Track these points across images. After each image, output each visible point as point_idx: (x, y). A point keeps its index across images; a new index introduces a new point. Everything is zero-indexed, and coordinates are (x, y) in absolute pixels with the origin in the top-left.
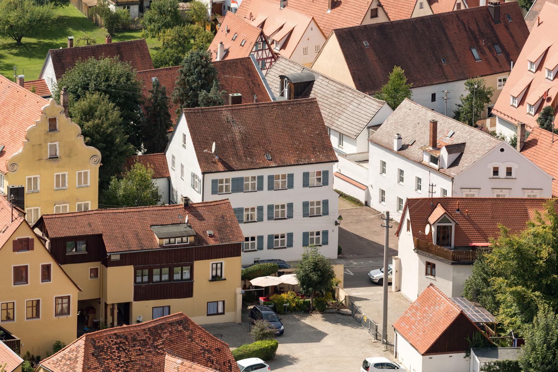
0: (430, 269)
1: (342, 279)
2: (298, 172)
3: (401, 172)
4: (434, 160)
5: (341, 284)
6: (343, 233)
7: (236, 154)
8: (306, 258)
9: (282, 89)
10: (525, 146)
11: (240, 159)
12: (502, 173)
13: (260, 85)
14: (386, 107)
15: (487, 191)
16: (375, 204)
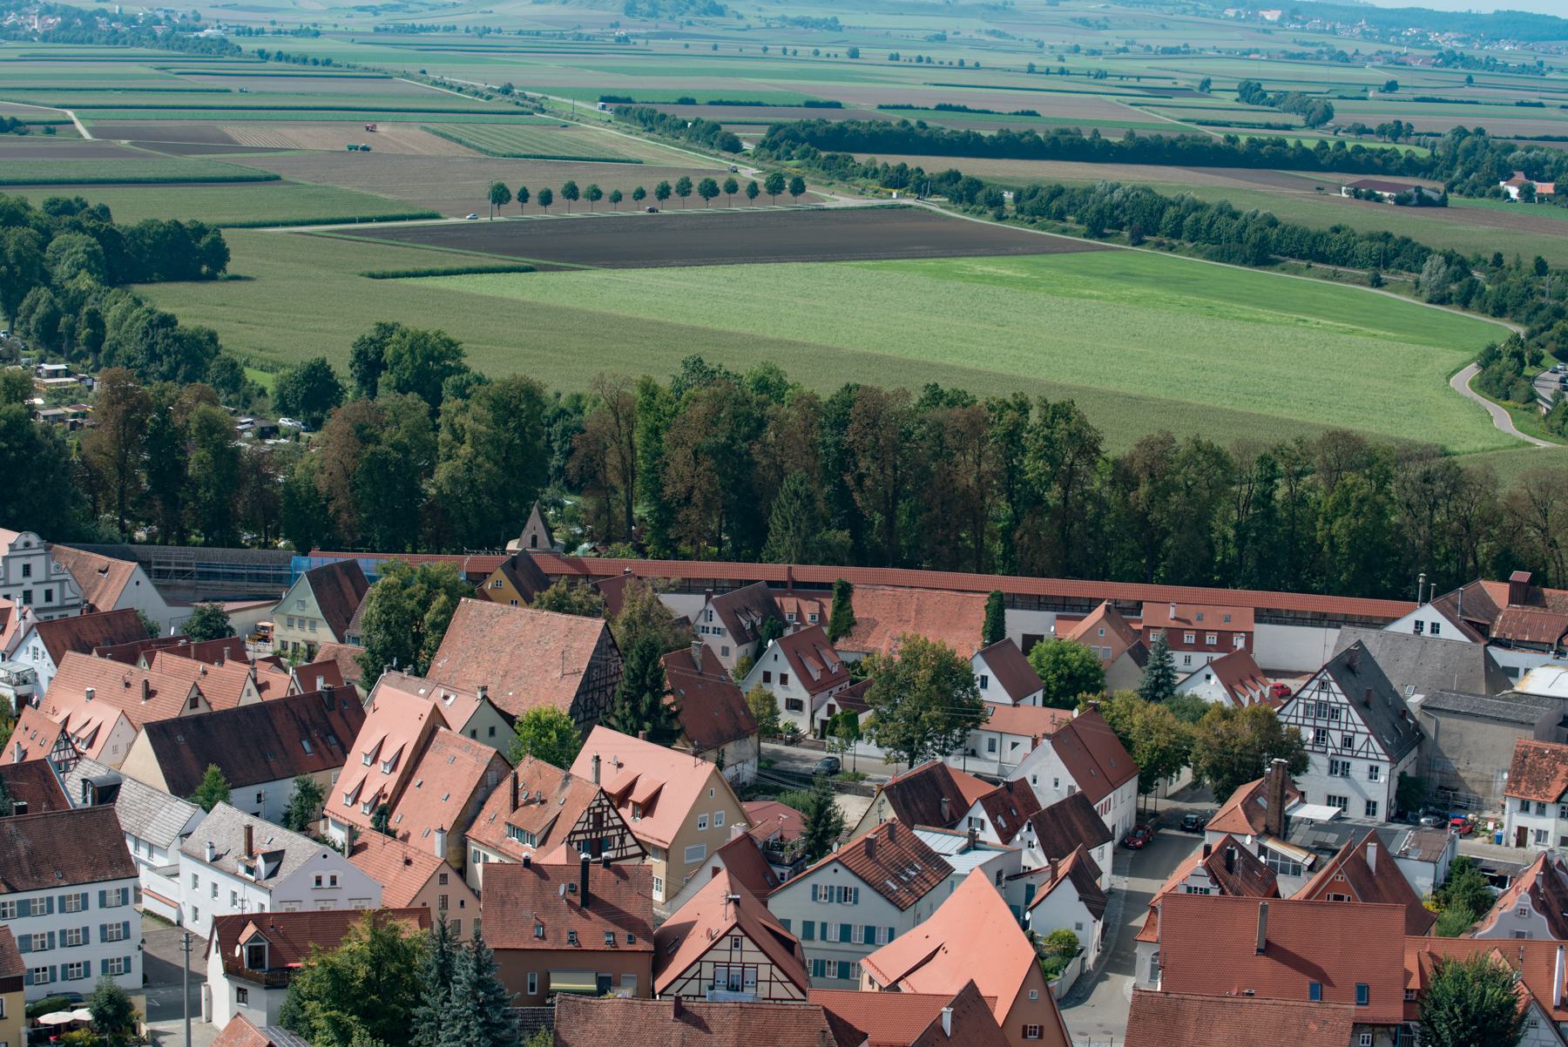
0: (241, 995)
1: (144, 1011)
2: (93, 891)
3: (215, 886)
4: (250, 870)
5: (144, 1017)
6: (148, 960)
7: (21, 873)
8: (99, 989)
9: (85, 793)
10: (354, 850)
11: (25, 878)
12: (326, 882)
13: (58, 791)
14: (201, 810)
15: (309, 903)
16: (188, 923)
